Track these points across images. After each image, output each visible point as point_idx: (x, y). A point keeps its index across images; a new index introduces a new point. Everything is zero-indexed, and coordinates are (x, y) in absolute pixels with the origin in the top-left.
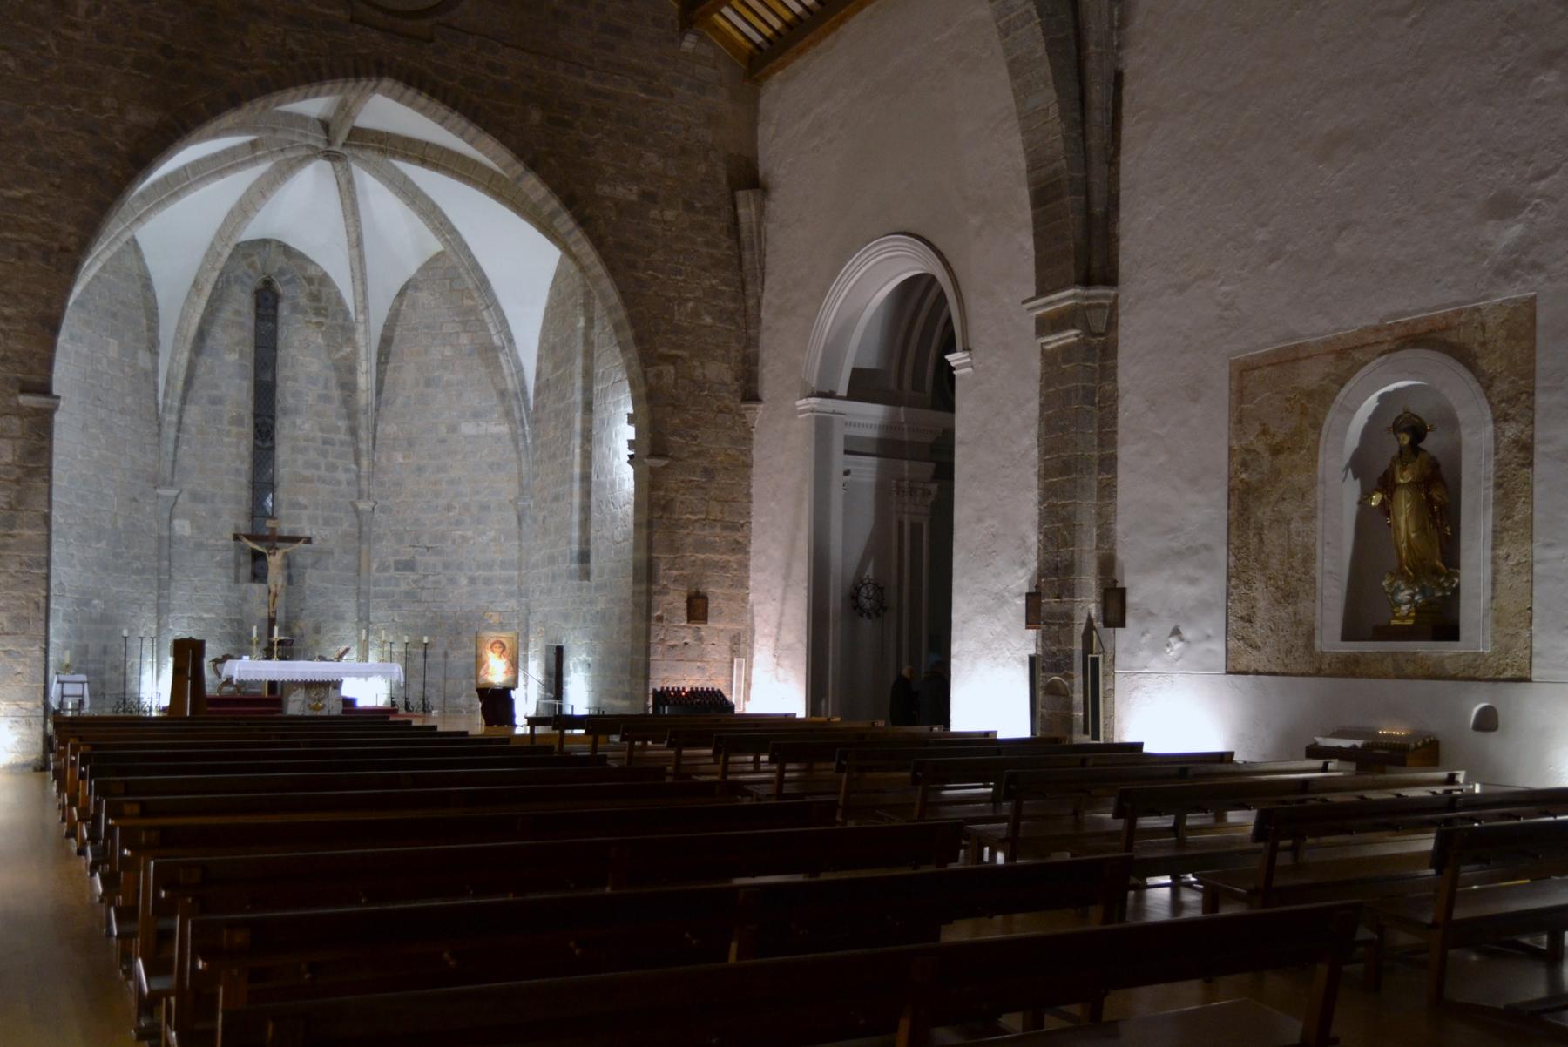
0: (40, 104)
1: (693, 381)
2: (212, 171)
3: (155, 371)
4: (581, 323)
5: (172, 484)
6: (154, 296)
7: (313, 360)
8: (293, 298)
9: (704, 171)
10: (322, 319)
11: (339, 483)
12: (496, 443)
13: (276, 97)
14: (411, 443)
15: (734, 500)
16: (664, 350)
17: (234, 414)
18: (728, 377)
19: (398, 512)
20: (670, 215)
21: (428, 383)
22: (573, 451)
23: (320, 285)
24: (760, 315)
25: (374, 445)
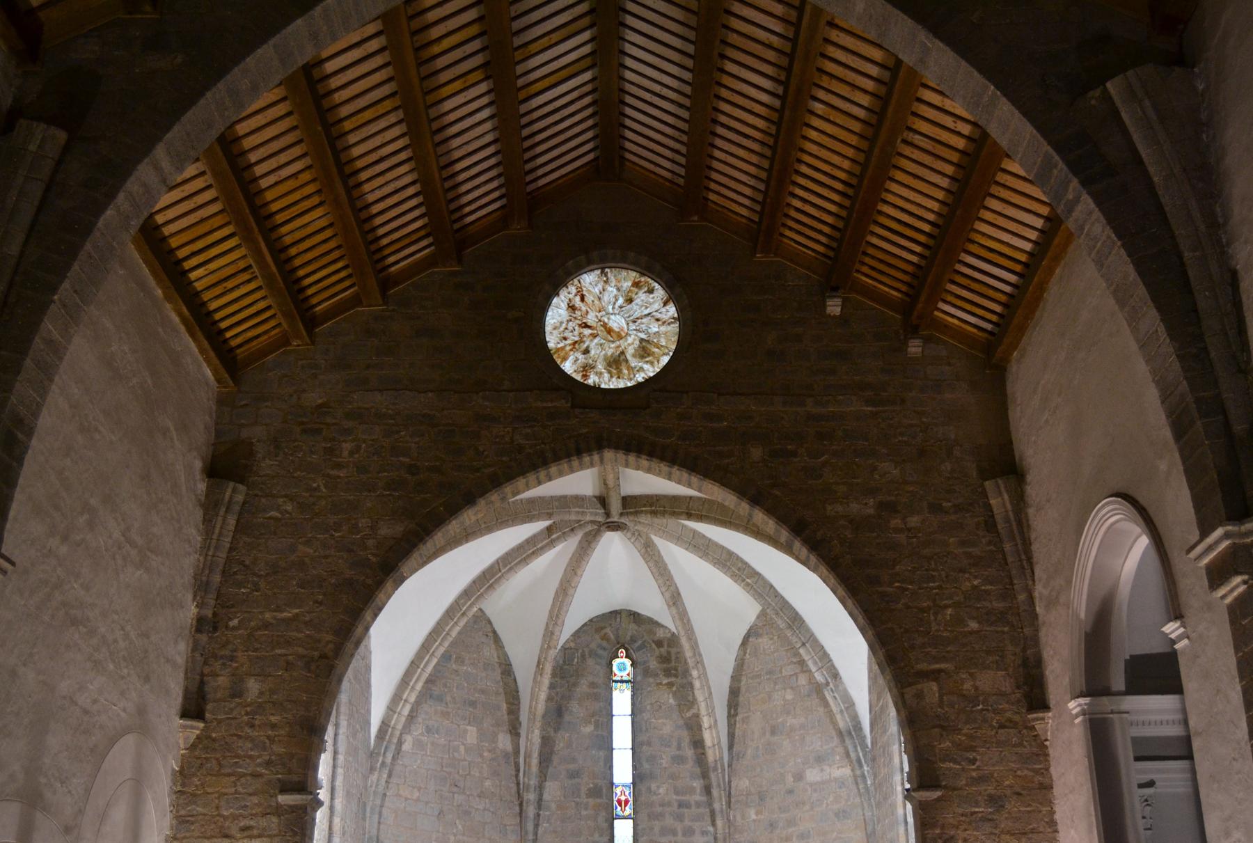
0: (310, 535)
1: (964, 695)
3: (517, 752)
6: (515, 680)
7: (665, 721)
8: (645, 662)
9: (949, 469)
10: (673, 679)
12: (840, 788)
13: (521, 482)
14: (762, 798)
15: (1033, 831)
16: (923, 666)
17: (592, 785)
18: (1007, 686)
20: (914, 521)
21: (773, 732)
23: (669, 646)
24: (1035, 610)
25: (729, 804)
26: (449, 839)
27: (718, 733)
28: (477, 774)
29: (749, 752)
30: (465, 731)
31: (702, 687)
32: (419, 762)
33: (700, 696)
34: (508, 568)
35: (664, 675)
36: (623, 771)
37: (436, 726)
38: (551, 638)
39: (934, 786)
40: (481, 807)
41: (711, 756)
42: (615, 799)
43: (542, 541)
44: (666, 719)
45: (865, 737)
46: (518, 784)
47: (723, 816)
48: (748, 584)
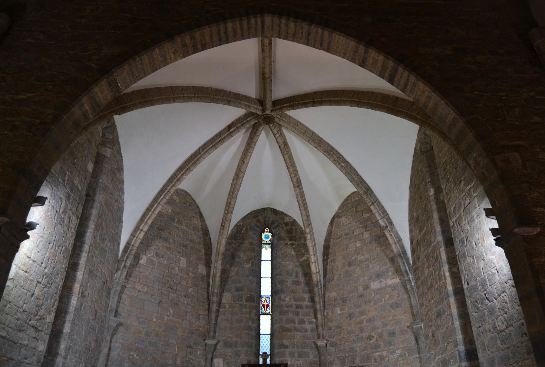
2: (211, 146)
4: (432, 192)
5: (214, 337)
6: (210, 239)
7: (289, 263)
8: (279, 233)
10: (294, 242)
11: (306, 330)
12: (393, 290)
14: (344, 301)
17: (249, 295)
19: (341, 345)
21: (350, 265)
22: (444, 275)
23: (291, 226)
26: (164, 318)
27: (318, 266)
28: (185, 284)
29: (335, 277)
30: (180, 260)
31: (311, 238)
32: (149, 271)
33: (309, 243)
34: (204, 151)
35: (289, 240)
36: (266, 289)
37: (162, 254)
38: (229, 206)
39: (531, 222)
40: (185, 302)
41: (315, 278)
42: (261, 304)
43: (225, 134)
44: (290, 261)
45: (408, 258)
46: (208, 293)
47: (321, 313)
48: (342, 166)
